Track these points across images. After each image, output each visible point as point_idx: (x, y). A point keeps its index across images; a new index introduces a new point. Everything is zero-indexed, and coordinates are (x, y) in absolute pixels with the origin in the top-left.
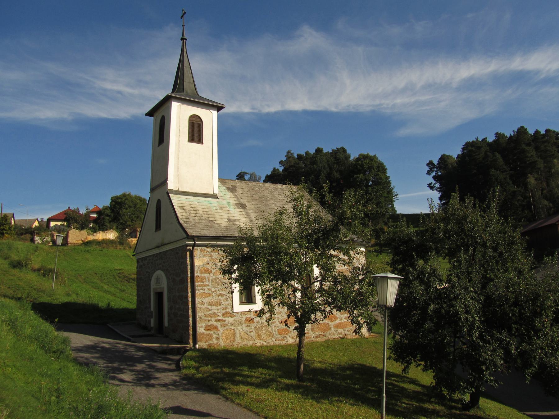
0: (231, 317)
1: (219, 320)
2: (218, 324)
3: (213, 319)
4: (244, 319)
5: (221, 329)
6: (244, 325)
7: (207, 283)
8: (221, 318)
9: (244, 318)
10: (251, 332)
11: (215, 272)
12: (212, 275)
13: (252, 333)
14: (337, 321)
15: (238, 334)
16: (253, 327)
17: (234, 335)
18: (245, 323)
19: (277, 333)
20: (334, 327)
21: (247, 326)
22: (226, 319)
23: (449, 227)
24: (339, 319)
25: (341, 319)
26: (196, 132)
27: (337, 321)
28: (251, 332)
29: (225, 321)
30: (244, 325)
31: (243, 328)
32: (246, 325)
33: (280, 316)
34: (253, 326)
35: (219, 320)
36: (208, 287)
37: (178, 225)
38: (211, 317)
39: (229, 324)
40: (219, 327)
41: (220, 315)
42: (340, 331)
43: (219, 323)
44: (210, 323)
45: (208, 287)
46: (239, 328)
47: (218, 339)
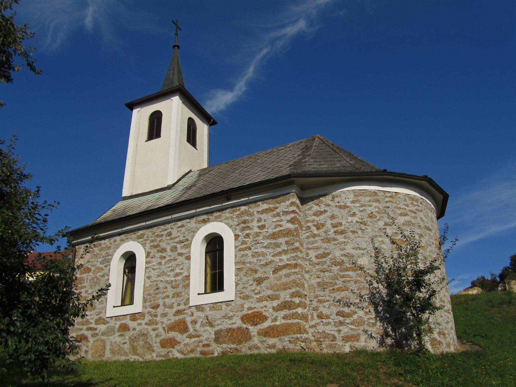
0: (104, 323)
1: (91, 329)
2: (88, 334)
3: (85, 327)
4: (117, 326)
5: (91, 340)
6: (117, 334)
7: (85, 285)
8: (93, 326)
9: (119, 323)
10: (125, 343)
11: (94, 271)
12: (91, 274)
13: (126, 345)
14: (266, 324)
15: (108, 348)
16: (127, 337)
17: (104, 347)
18: (119, 331)
19: (159, 345)
20: (259, 334)
21: (121, 335)
22: (99, 326)
23: (277, 380)
24: (269, 320)
25: (275, 320)
26: (155, 129)
27: (266, 324)
28: (125, 343)
29: (96, 329)
30: (117, 334)
31: (116, 338)
32: (120, 333)
33: (165, 320)
34: (128, 334)
35: (91, 329)
36: (86, 289)
37: (342, 163)
38: (84, 325)
39: (100, 334)
40: (89, 336)
41: (93, 321)
42: (271, 341)
43: (90, 332)
44: (82, 332)
45: (86, 289)
46: (110, 337)
47: (86, 352)
